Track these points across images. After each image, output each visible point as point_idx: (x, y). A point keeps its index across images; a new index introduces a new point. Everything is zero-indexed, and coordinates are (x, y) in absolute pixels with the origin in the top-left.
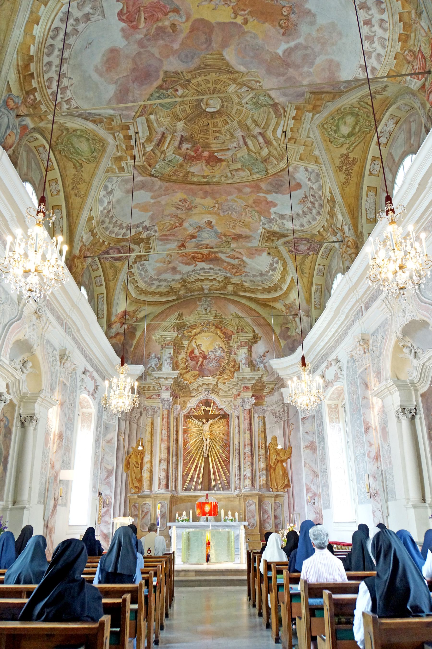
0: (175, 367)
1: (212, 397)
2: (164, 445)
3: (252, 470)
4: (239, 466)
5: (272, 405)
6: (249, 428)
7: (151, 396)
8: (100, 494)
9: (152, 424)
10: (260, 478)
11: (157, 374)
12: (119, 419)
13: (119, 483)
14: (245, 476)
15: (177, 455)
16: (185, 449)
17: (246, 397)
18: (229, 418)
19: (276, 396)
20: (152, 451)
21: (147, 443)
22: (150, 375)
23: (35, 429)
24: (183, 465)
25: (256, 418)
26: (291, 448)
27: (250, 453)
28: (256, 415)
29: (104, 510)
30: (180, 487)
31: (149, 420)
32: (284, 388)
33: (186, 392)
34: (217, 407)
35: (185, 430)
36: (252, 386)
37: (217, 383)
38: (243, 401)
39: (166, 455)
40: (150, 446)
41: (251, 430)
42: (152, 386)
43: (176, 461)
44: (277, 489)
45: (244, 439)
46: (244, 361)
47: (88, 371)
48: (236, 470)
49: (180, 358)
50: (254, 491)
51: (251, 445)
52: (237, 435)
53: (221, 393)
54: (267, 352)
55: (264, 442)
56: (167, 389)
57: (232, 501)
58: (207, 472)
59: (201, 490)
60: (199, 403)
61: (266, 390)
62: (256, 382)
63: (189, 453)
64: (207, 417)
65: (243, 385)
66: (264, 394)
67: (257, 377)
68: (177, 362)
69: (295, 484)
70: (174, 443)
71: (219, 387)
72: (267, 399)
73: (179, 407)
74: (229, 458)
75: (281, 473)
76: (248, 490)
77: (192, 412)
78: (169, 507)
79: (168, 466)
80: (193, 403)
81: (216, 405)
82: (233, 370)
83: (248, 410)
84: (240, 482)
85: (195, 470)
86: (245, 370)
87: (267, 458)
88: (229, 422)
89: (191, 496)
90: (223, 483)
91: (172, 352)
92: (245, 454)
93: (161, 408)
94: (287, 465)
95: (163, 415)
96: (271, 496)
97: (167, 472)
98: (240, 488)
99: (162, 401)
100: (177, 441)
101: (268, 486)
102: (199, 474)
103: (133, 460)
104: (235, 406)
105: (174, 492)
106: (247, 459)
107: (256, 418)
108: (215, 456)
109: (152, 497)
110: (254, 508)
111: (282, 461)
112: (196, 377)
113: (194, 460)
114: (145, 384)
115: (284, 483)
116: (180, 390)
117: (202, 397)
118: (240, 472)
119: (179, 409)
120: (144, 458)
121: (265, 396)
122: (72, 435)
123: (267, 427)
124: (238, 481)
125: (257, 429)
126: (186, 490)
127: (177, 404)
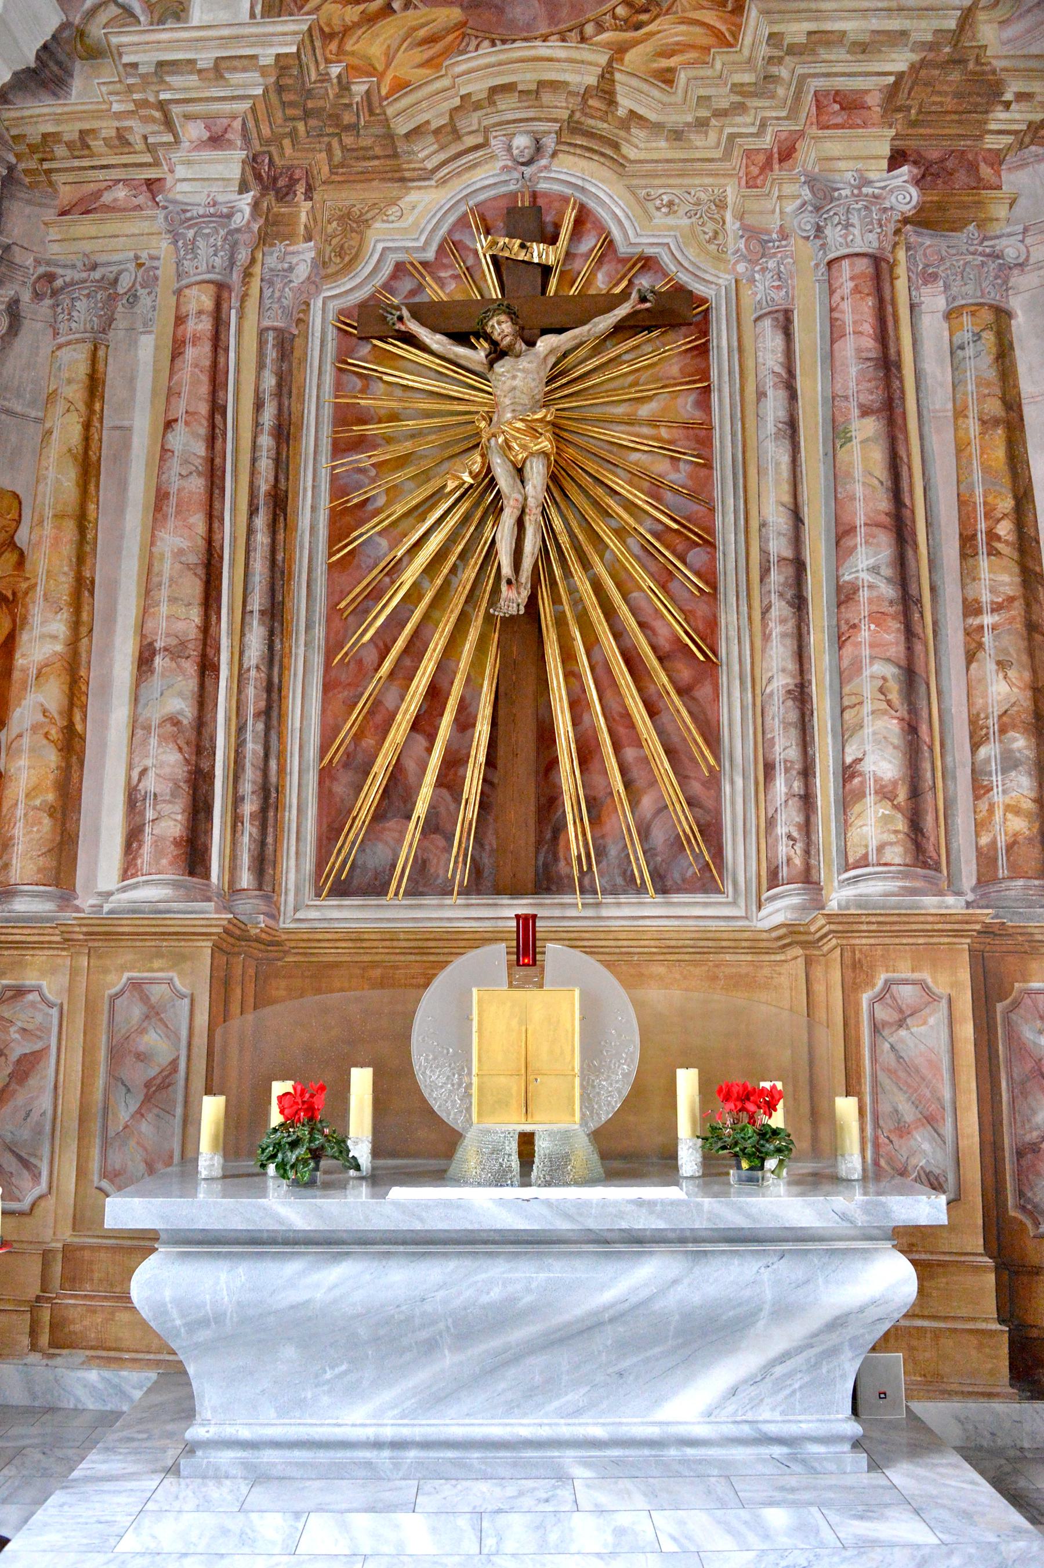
1: (568, 174)
2: (180, 540)
3: (911, 729)
4: (801, 695)
6: (875, 398)
7: (98, 194)
9: (95, 385)
10: (980, 789)
11: (142, 45)
14: (848, 773)
15: (276, 614)
16: (343, 566)
17: (846, 174)
18: (703, 327)
20: (82, 587)
21: (48, 529)
22: (95, 53)
24: (328, 687)
25: (933, 326)
27: (888, 591)
28: (934, 302)
30: (295, 865)
31: (75, 361)
33: (363, 154)
34: (609, 244)
35: (347, 417)
36: (893, 91)
37: (607, 75)
38: (823, 195)
39: (195, 615)
40: (67, 550)
41: (890, 409)
42: (108, 128)
43: (274, 658)
45: (837, 477)
48: (775, 727)
50: (930, 903)
52: (777, 454)
53: (638, 147)
55: (1006, 504)
56: (216, 141)
57: (739, 982)
58: (525, 738)
60: (462, 222)
61: (1007, 119)
62: (923, 63)
63: (375, 594)
65: (815, 84)
66: (992, 142)
70: (261, 521)
71: (625, 103)
73: (303, 256)
76: (875, 888)
77: (406, 285)
78: (202, 1019)
79: (204, 700)
80: (413, 221)
81: (602, 229)
83: (863, 265)
84: (807, 827)
85: (424, 725)
88: (702, 351)
89: (390, 937)
90: (659, 836)
92: (844, 595)
93: (166, 271)
95: (180, 320)
97: (199, 746)
98: (808, 878)
99: (180, 223)
100: (280, 504)
102: (454, 763)
104: (751, 232)
105: (249, 907)
106: (865, 634)
107: (933, 326)
108: (597, 615)
109: (68, 942)
112: (440, 49)
113: (415, 649)
114: (58, 119)
117: (488, 178)
118: (805, 741)
119: (302, 271)
120: (24, 638)
121: (997, 159)
125: (940, 399)
126: (342, 889)
127: (290, 237)
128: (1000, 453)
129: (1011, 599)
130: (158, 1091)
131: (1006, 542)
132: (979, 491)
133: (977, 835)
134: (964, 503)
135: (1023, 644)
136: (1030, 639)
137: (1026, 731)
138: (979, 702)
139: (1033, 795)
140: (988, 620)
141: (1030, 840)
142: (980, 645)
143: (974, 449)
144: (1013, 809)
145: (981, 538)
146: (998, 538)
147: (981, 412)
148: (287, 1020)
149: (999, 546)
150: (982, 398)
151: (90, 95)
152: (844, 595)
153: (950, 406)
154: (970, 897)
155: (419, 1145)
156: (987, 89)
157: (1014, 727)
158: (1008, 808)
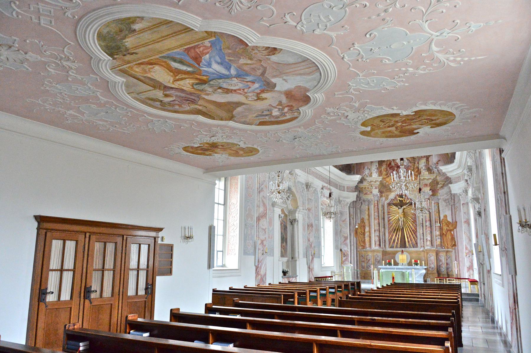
0: (380, 174)
2: (376, 222)
4: (423, 233)
5: (443, 195)
8: (341, 250)
9: (369, 209)
12: (349, 207)
13: (352, 243)
15: (384, 227)
17: (426, 191)
19: (445, 189)
20: (369, 225)
23: (297, 225)
28: (433, 202)
29: (344, 259)
31: (367, 207)
32: (451, 183)
35: (388, 212)
46: (424, 168)
47: (324, 187)
49: (383, 168)
51: (430, 221)
54: (439, 161)
56: (376, 188)
59: (400, 247)
61: (439, 186)
64: (401, 204)
67: (432, 178)
68: (381, 171)
69: (459, 244)
72: (440, 191)
73: (384, 198)
74: (416, 229)
75: (450, 237)
79: (380, 234)
80: (392, 196)
82: (417, 174)
85: (396, 236)
86: (425, 174)
87: (441, 229)
91: (377, 164)
92: (426, 226)
94: (454, 232)
96: (444, 251)
97: (379, 237)
100: (384, 219)
101: (441, 246)
102: (398, 238)
103: (359, 231)
110: (433, 258)
111: (451, 231)
116: (384, 188)
122: (318, 222)
123: (440, 209)
124: (422, 243)
125: (433, 211)
130: (379, 262)
148: (387, 257)
151: (365, 184)
152: (426, 226)
155: (396, 264)
156: (438, 183)
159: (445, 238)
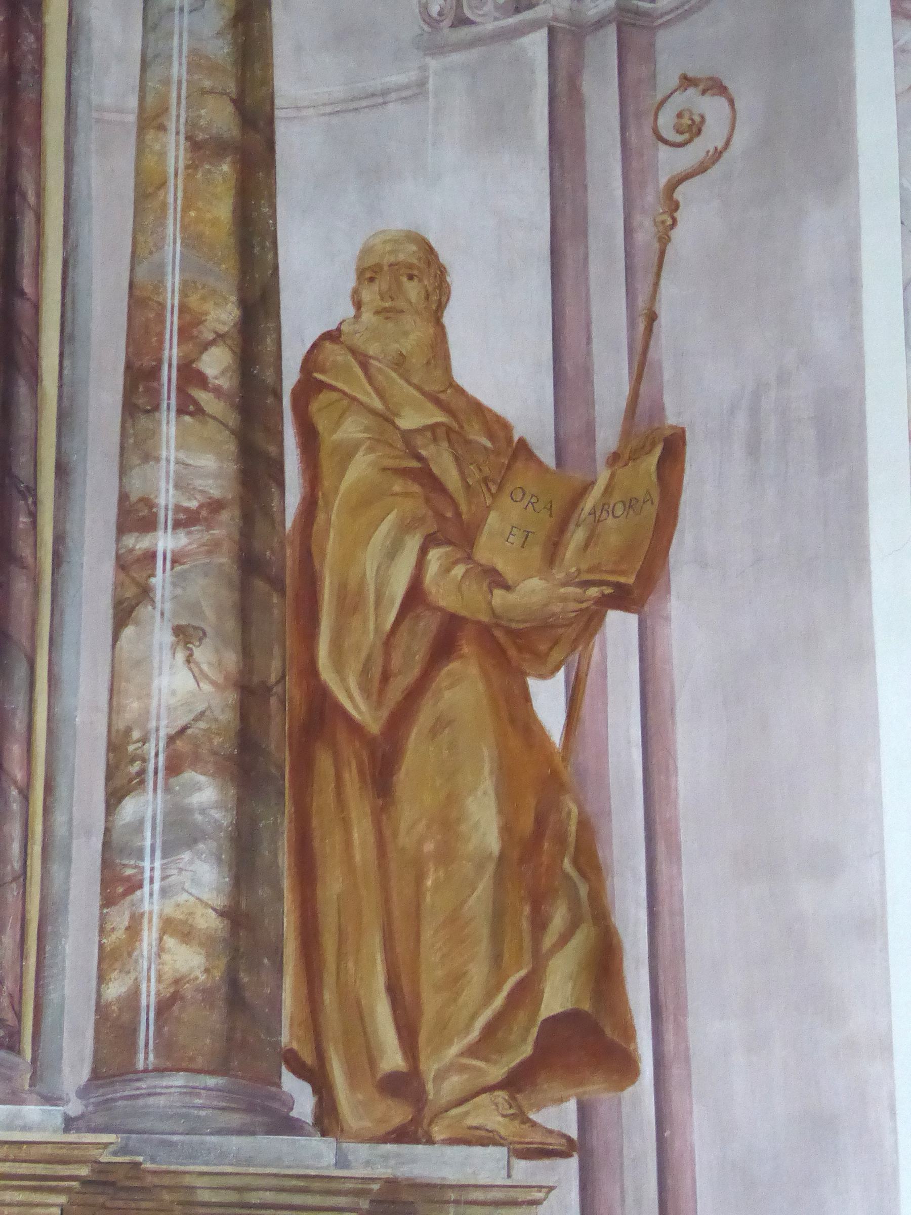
10: (116, 884)
26: (673, 448)
44: (404, 1086)
55: (224, 315)
69: (712, 1029)
75: (484, 824)
87: (269, 581)
94: (596, 703)
101: (244, 1032)
111: (516, 648)
115: (527, 992)
123: (301, 76)
125: (113, 87)
128: (223, 210)
129: (215, 506)
131: (217, 391)
132: (173, 281)
133: (102, 979)
134: (141, 302)
135: (228, 597)
136: (244, 589)
137: (219, 772)
138: (133, 706)
139: (220, 901)
140: (165, 542)
141: (207, 993)
142: (146, 593)
143: (174, 195)
144: (177, 928)
145: (169, 376)
146: (202, 381)
147: (193, 124)
149: (203, 397)
150: (198, 95)
153: (133, 102)
154: (75, 1107)
157: (195, 760)
158: (169, 926)
159: (350, 838)
